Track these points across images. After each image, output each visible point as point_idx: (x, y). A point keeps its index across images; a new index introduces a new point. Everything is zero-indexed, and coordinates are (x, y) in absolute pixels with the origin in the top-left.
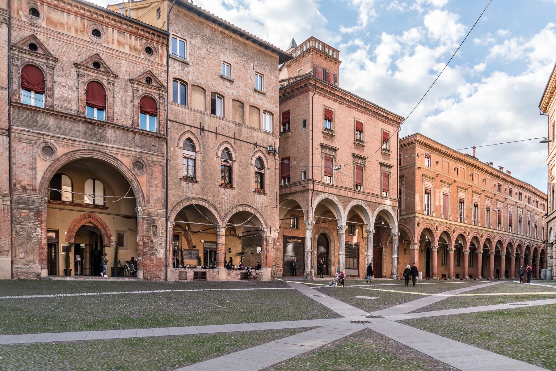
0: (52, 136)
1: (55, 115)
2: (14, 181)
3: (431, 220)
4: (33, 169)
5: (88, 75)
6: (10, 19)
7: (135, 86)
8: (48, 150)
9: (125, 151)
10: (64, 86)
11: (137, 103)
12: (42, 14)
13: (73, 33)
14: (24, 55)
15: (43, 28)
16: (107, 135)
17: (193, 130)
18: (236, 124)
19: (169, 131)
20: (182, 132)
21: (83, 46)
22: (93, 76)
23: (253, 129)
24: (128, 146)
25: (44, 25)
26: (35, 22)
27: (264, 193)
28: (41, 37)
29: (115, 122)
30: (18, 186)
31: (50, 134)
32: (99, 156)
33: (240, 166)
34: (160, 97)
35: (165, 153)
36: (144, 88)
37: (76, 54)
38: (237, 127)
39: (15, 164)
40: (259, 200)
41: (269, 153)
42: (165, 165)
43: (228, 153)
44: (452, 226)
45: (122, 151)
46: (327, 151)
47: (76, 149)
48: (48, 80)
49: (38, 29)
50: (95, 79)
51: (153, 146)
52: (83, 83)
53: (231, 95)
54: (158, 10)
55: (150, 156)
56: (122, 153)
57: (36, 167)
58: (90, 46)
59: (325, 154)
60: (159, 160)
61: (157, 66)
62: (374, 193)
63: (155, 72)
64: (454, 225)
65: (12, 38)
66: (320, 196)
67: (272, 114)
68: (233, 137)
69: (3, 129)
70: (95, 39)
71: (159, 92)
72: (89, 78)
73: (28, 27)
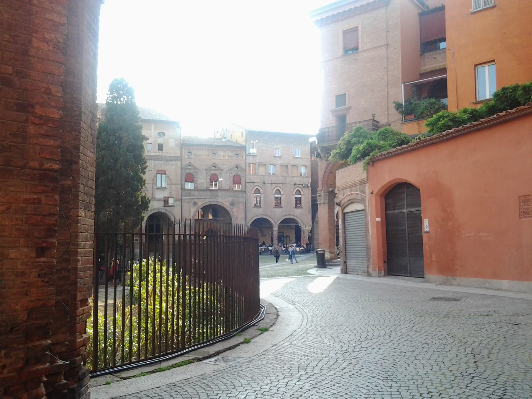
4: (189, 212)
7: (231, 172)
8: (195, 204)
11: (231, 179)
17: (259, 184)
18: (283, 176)
27: (301, 207)
28: (192, 162)
29: (222, 189)
40: (298, 211)
41: (304, 187)
42: (245, 202)
43: (278, 192)
57: (191, 211)
65: (182, 165)
67: (306, 166)
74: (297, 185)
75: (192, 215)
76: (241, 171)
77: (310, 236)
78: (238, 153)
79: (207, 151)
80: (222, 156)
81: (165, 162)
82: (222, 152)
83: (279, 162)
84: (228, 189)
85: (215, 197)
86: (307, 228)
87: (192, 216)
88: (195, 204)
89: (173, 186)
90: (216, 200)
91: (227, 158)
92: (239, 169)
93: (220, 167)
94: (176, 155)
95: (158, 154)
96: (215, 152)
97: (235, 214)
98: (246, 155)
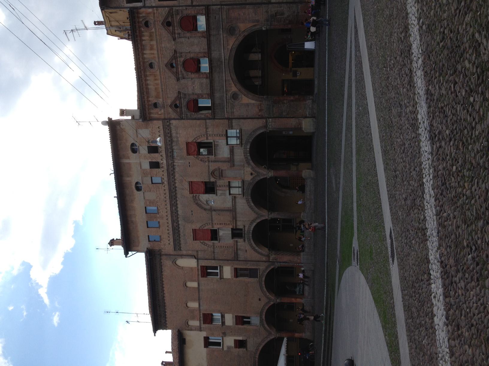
0: (226, 94)
1: (213, 93)
2: (257, 116)
5: (181, 72)
6: (166, 119)
8: (235, 96)
9: (225, 43)
10: (193, 87)
11: (188, 35)
12: (156, 101)
14: (183, 111)
15: (163, 100)
16: (216, 57)
19: (200, 4)
22: (181, 68)
25: (161, 100)
26: (161, 105)
28: (169, 102)
29: (206, 51)
30: (259, 114)
31: (225, 95)
32: (232, 62)
34: (178, 14)
36: (176, 28)
39: (247, 116)
45: (225, 45)
47: (230, 78)
48: (193, 97)
49: (165, 103)
51: (215, 19)
52: (187, 75)
54: (111, 13)
58: (162, 70)
60: (225, 13)
63: (161, 19)
69: (229, 122)
70: (156, 66)
71: (174, 15)
72: (183, 71)
73: (166, 109)
75: (253, 102)
76: (172, 17)
78: (143, 22)
79: (148, 78)
80: (152, 52)
81: (174, 144)
82: (145, 52)
84: (206, 39)
85: (222, 62)
87: (256, 100)
88: (235, 96)
89: (210, 131)
91: (154, 43)
92: (170, 20)
93: (171, 55)
94: (161, 127)
95: (164, 153)
97: (249, 25)
98: (144, 7)
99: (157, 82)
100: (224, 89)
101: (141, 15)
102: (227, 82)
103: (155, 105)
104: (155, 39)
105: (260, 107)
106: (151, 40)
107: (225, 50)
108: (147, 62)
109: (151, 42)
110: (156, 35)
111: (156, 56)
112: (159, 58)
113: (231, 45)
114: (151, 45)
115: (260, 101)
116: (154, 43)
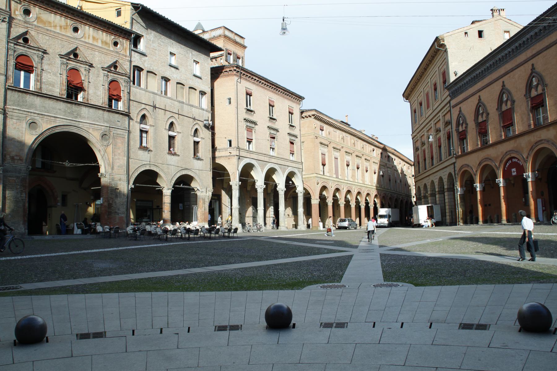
3: (327, 179)
10: (49, 72)
13: (58, 30)
17: (147, 107)
20: (140, 109)
21: (65, 40)
23: (192, 106)
24: (97, 121)
33: (183, 136)
35: (127, 127)
37: (60, 46)
38: (180, 105)
44: (342, 183)
45: (93, 125)
46: (249, 124)
49: (31, 26)
50: (74, 67)
51: (118, 121)
53: (175, 78)
55: (116, 129)
56: (93, 128)
59: (247, 126)
60: (122, 133)
61: (122, 57)
62: (284, 157)
64: (344, 182)
66: (244, 161)
68: (177, 113)
73: (23, 24)
74: (196, 122)
77: (182, 209)
80: (91, 38)
83: (175, 76)
85: (76, 117)
86: (208, 194)
90: (76, 124)
91: (100, 44)
96: (79, 27)
99: (58, 28)
100: (45, 112)
101: (125, 42)
102: (53, 119)
103: (27, 12)
104: (103, 47)
105: (18, 158)
106: (102, 42)
107: (88, 125)
108: (81, 27)
109: (101, 41)
110: (107, 50)
111: (87, 41)
112: (86, 43)
113: (92, 133)
114: (98, 39)
115: (26, 160)
116: (100, 44)
